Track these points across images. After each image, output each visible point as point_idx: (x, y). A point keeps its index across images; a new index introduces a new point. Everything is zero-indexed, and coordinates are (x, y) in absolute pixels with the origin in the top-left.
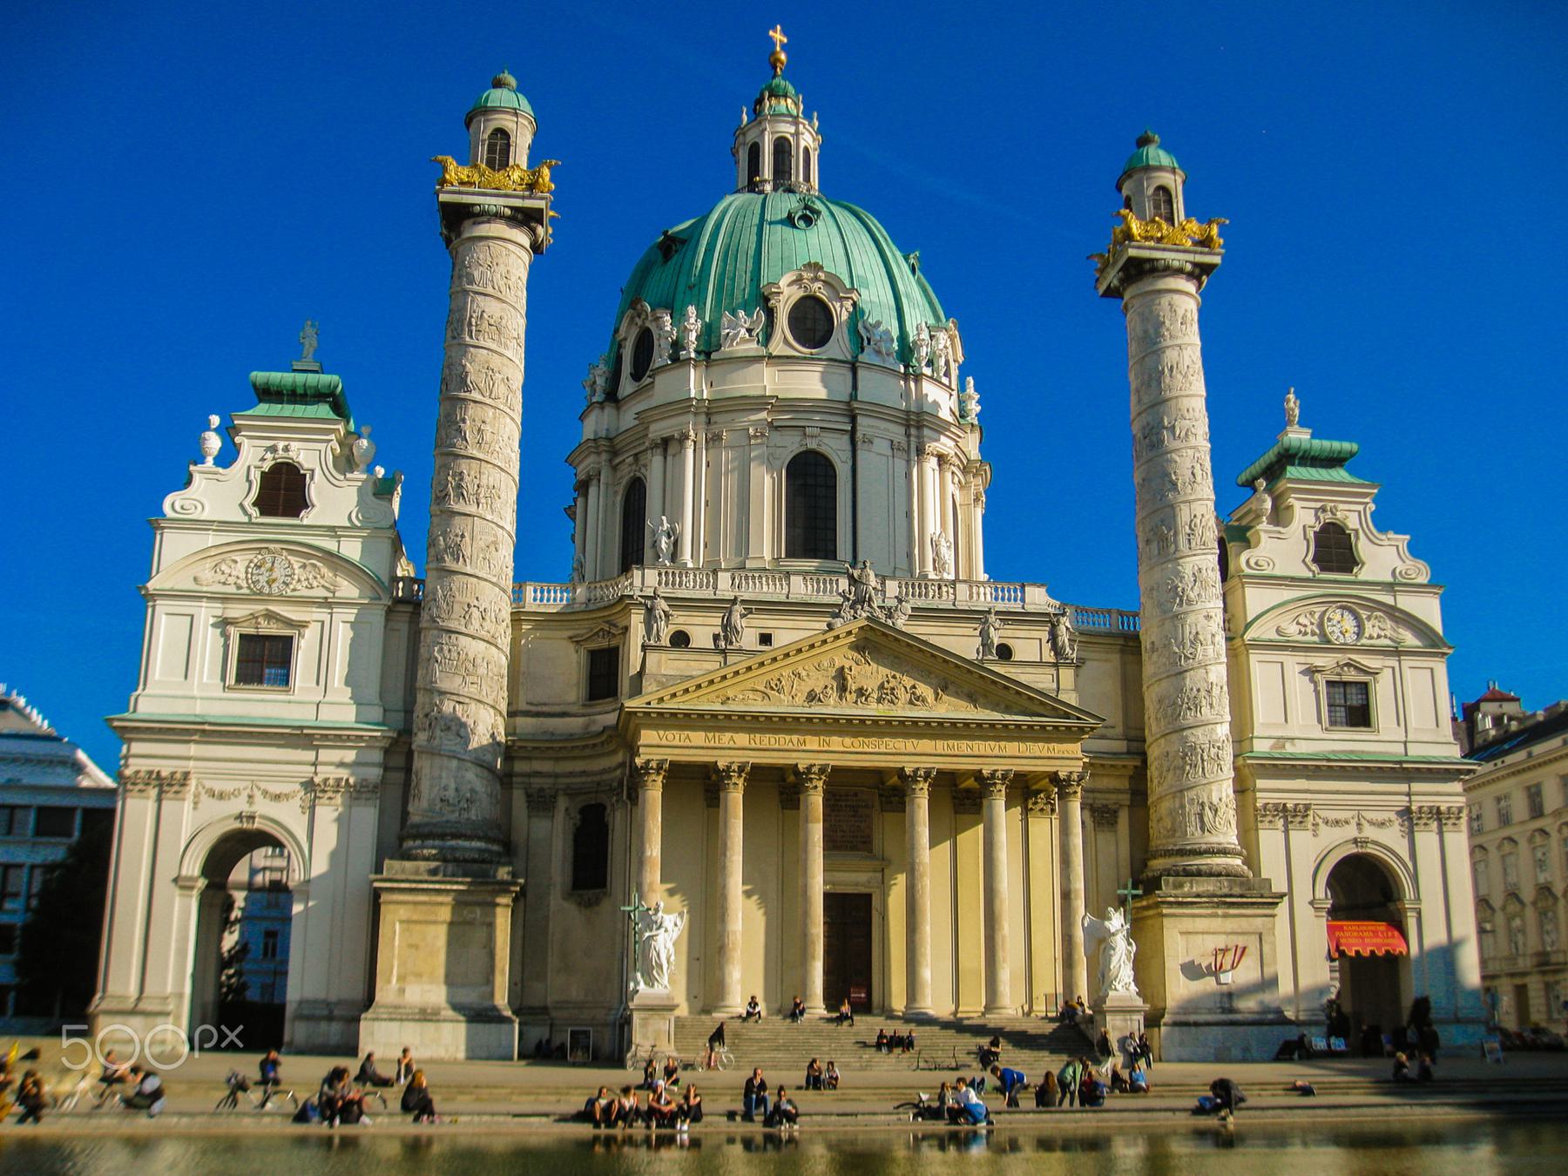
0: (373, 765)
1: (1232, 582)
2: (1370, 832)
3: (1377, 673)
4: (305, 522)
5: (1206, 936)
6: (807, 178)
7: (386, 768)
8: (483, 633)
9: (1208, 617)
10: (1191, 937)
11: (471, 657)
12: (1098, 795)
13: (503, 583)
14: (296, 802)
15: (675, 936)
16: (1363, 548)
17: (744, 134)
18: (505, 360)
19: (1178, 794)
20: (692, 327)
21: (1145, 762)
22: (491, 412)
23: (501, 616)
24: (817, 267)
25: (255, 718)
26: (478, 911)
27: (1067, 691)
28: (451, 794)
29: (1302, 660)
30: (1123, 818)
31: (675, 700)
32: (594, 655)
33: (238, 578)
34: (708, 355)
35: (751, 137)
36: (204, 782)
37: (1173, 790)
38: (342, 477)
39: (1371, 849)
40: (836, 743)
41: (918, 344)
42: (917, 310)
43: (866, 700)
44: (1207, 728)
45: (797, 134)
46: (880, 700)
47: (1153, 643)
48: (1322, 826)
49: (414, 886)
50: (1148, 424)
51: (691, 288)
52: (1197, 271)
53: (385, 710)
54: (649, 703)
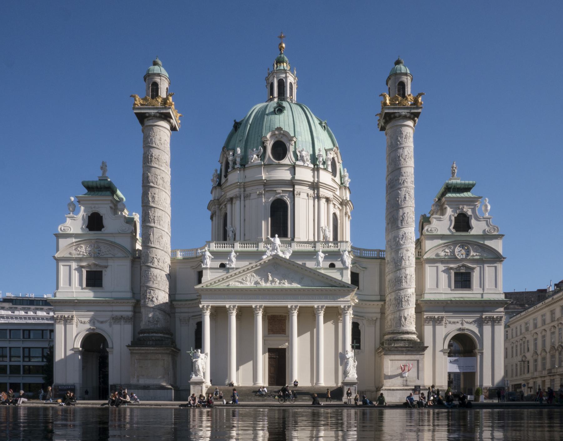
1: (423, 237)
4: (105, 232)
10: (394, 361)
11: (155, 275)
13: (165, 250)
21: (385, 303)
26: (160, 356)
33: (83, 252)
34: (244, 166)
36: (79, 318)
37: (392, 312)
39: (466, 332)
41: (319, 155)
42: (321, 144)
43: (275, 283)
45: (286, 77)
47: (388, 261)
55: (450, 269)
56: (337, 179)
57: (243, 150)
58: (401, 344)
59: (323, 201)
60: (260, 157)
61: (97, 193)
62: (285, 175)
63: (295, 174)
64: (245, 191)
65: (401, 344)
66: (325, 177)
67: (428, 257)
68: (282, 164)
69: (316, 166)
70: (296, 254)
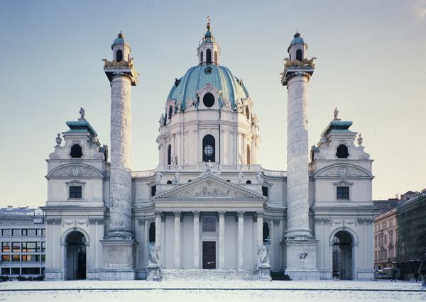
6: (216, 60)
7: (105, 216)
14: (86, 225)
16: (350, 151)
30: (281, 222)
32: (152, 187)
40: (202, 205)
45: (213, 48)
48: (333, 224)
53: (105, 203)
56: (250, 120)
59: (240, 137)
61: (77, 130)
65: (298, 239)
66: (242, 118)
70: (223, 173)
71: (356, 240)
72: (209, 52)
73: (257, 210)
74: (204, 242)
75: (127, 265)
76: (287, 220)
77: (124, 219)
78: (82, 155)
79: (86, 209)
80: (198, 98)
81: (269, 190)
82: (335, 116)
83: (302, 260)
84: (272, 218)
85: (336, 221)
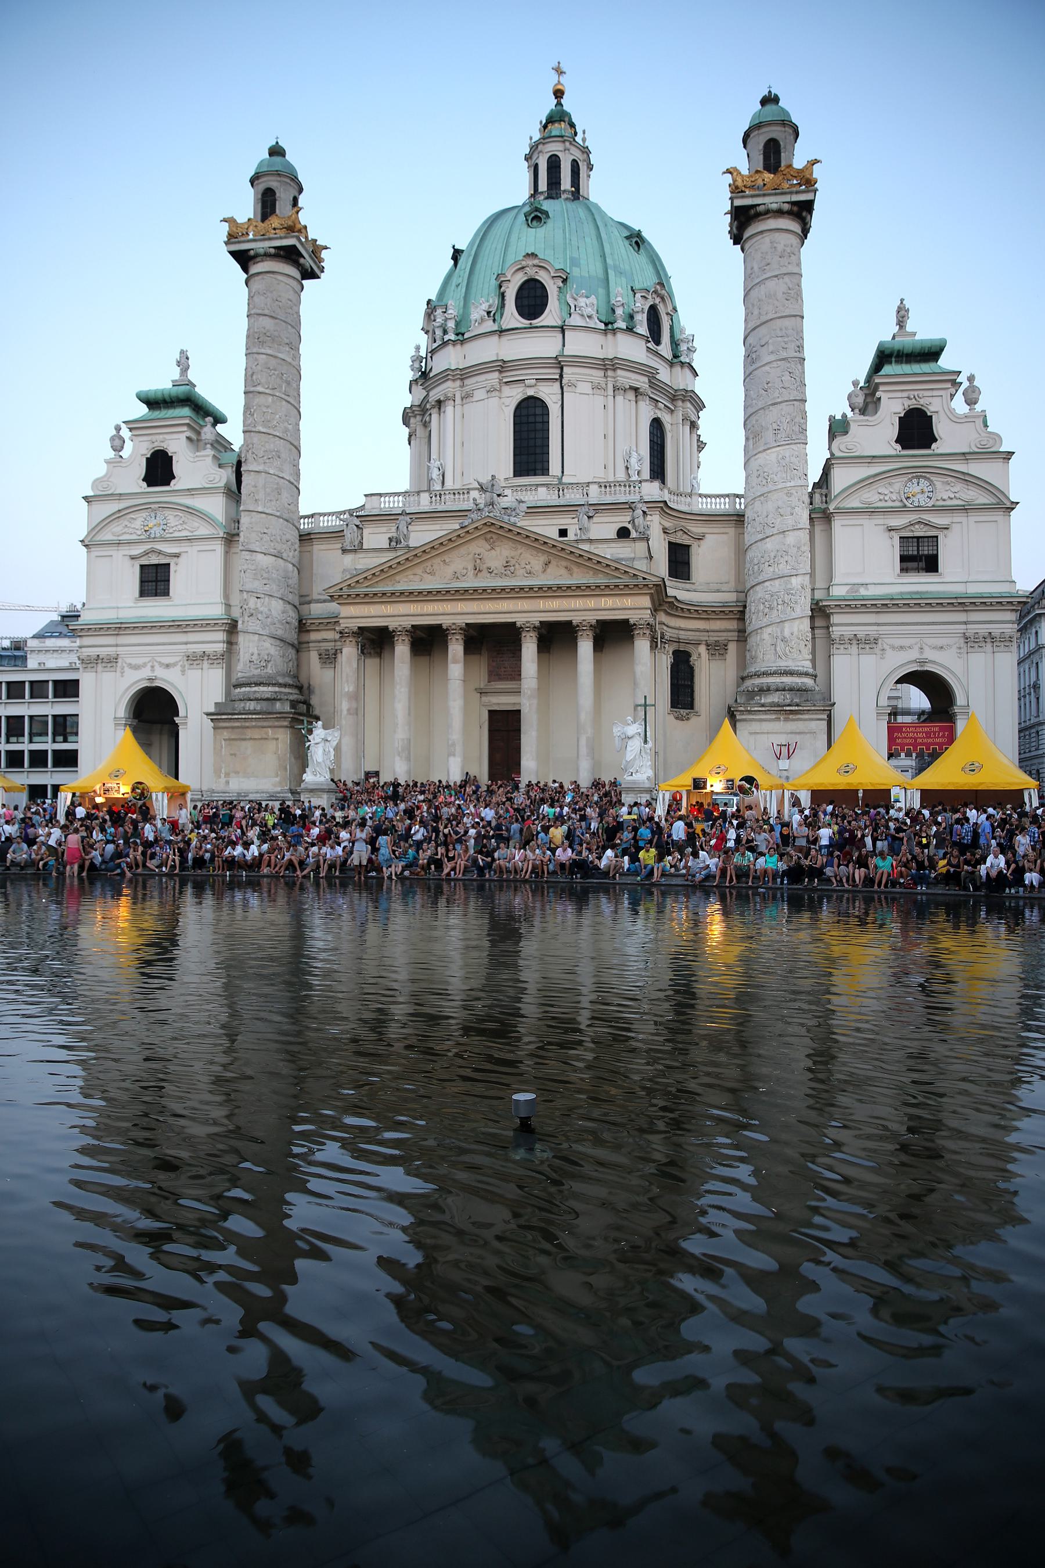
0: (219, 642)
2: (929, 654)
3: (947, 528)
4: (176, 488)
5: (770, 735)
7: (230, 643)
8: (272, 551)
9: (789, 494)
10: (759, 736)
12: (712, 634)
13: (285, 516)
14: (178, 668)
15: (335, 743)
16: (939, 427)
17: (531, 158)
18: (280, 361)
19: (759, 631)
20: (450, 316)
21: (745, 607)
22: (270, 399)
23: (288, 537)
24: (533, 255)
25: (152, 617)
27: (640, 559)
28: (255, 658)
29: (881, 522)
31: (358, 585)
34: (463, 334)
35: (533, 162)
38: (192, 455)
42: (624, 280)
44: (782, 580)
46: (501, 575)
48: (889, 652)
49: (230, 717)
50: (750, 345)
51: (457, 286)
52: (795, 209)
53: (228, 606)
54: (341, 589)
55: (890, 530)
57: (462, 303)
58: (774, 698)
60: (494, 314)
62: (544, 346)
63: (564, 346)
64: (462, 386)
65: (774, 698)
67: (841, 505)
68: (537, 327)
69: (610, 327)
71: (960, 700)
72: (554, 164)
73: (633, 617)
74: (490, 711)
75: (277, 779)
76: (746, 641)
77: (270, 648)
78: (174, 477)
79: (178, 626)
80: (503, 296)
81: (694, 550)
82: (901, 323)
83: (784, 764)
84: (704, 637)
85: (898, 642)
